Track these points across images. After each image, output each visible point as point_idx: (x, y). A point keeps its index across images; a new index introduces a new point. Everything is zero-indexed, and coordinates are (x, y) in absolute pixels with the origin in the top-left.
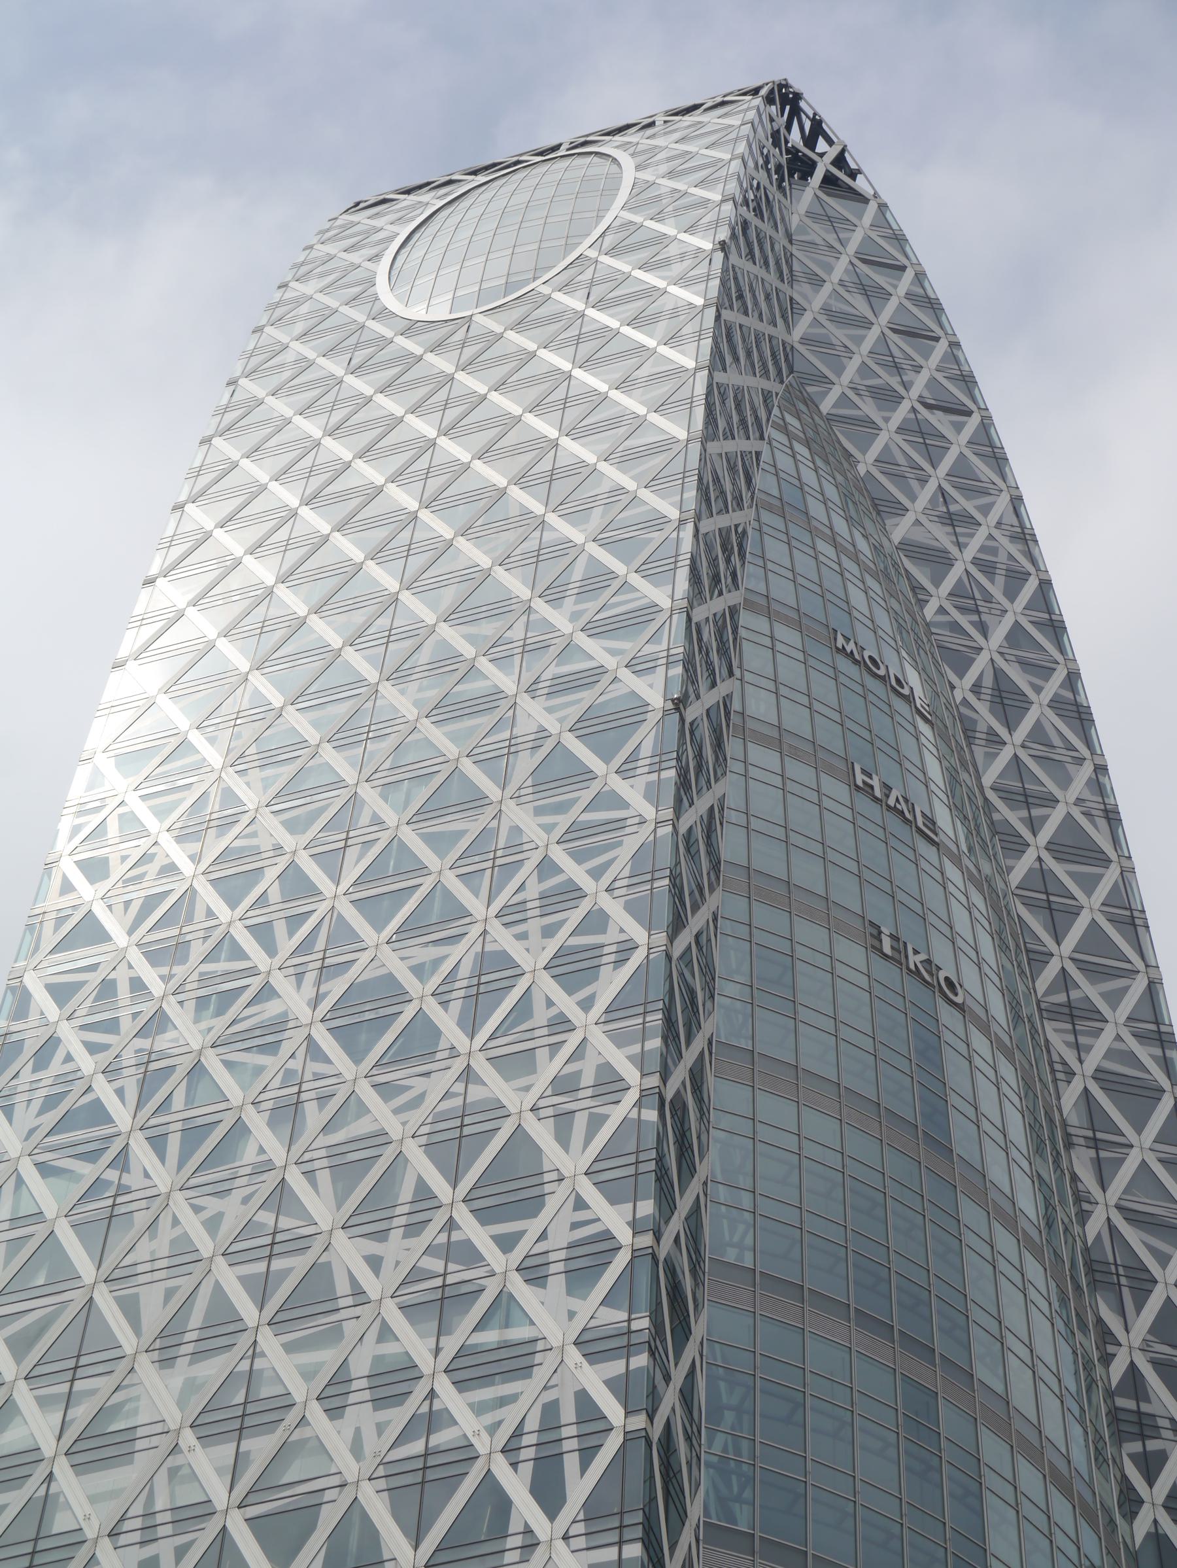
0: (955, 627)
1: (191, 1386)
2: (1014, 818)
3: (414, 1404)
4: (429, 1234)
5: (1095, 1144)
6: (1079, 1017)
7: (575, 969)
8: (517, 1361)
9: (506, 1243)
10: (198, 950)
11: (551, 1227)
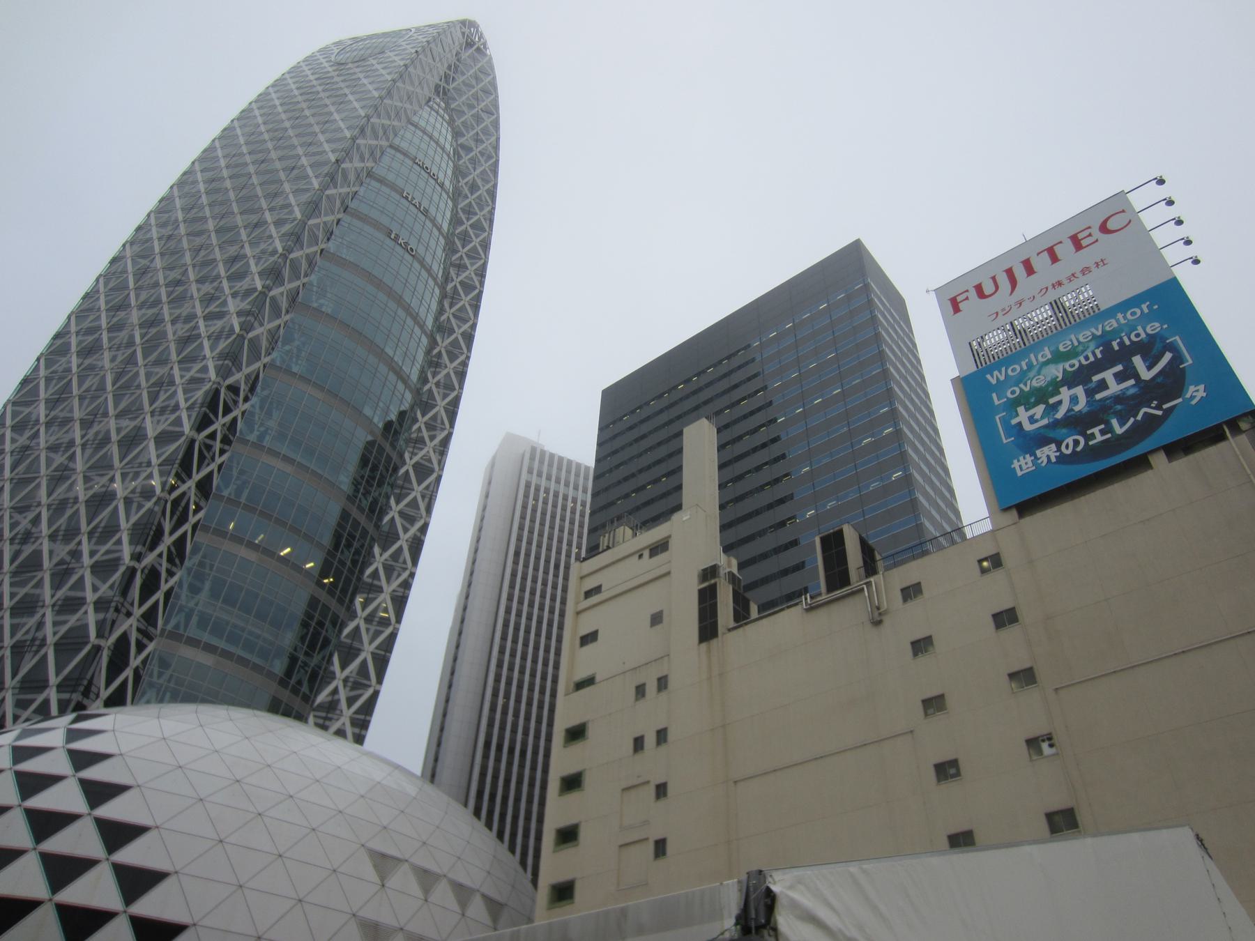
2: (463, 217)
5: (453, 298)
6: (461, 267)
8: (220, 315)
11: (244, 285)
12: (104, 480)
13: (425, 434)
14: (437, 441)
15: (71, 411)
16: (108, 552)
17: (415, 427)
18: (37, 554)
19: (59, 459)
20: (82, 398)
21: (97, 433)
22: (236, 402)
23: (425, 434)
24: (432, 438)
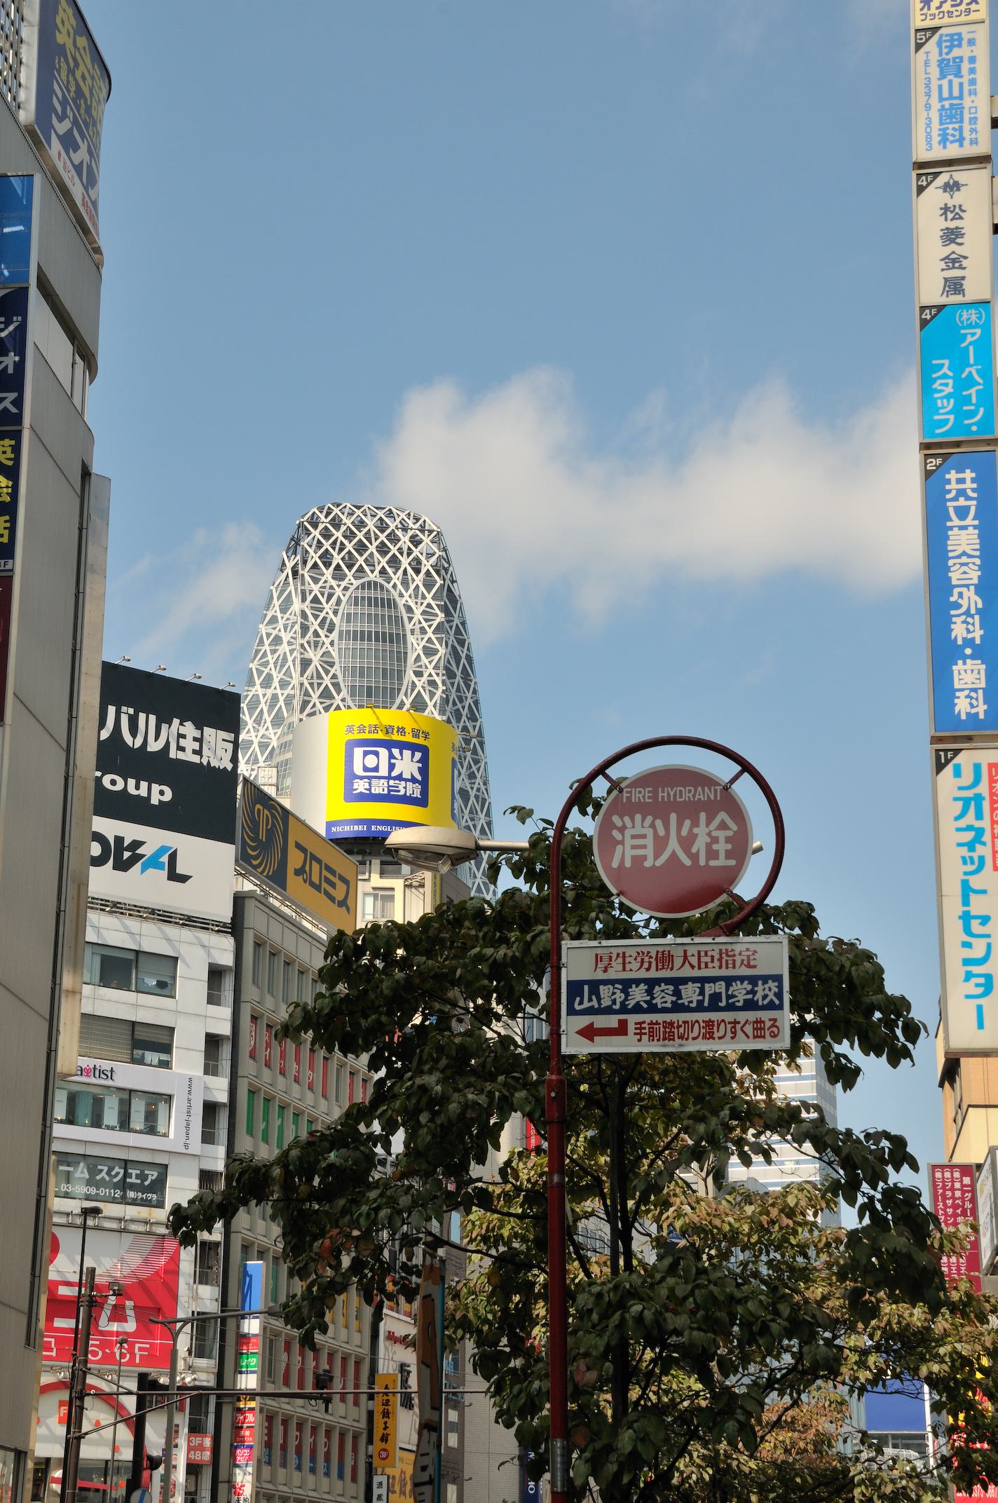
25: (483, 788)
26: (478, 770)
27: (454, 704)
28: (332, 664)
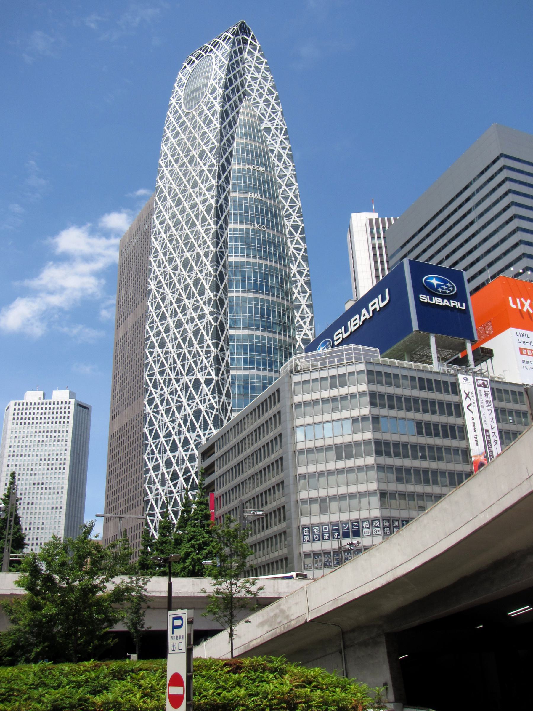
0: (272, 144)
1: (174, 321)
3: (195, 323)
4: (195, 299)
7: (206, 255)
9: (202, 299)
10: (168, 253)
11: (206, 297)
12: (194, 404)
13: (301, 322)
14: (307, 324)
15: (169, 375)
16: (209, 434)
17: (296, 321)
18: (186, 438)
19: (176, 398)
20: (170, 369)
21: (183, 384)
22: (224, 354)
23: (301, 322)
24: (305, 323)
25: (280, 123)
26: (276, 116)
27: (258, 90)
28: (179, 100)
